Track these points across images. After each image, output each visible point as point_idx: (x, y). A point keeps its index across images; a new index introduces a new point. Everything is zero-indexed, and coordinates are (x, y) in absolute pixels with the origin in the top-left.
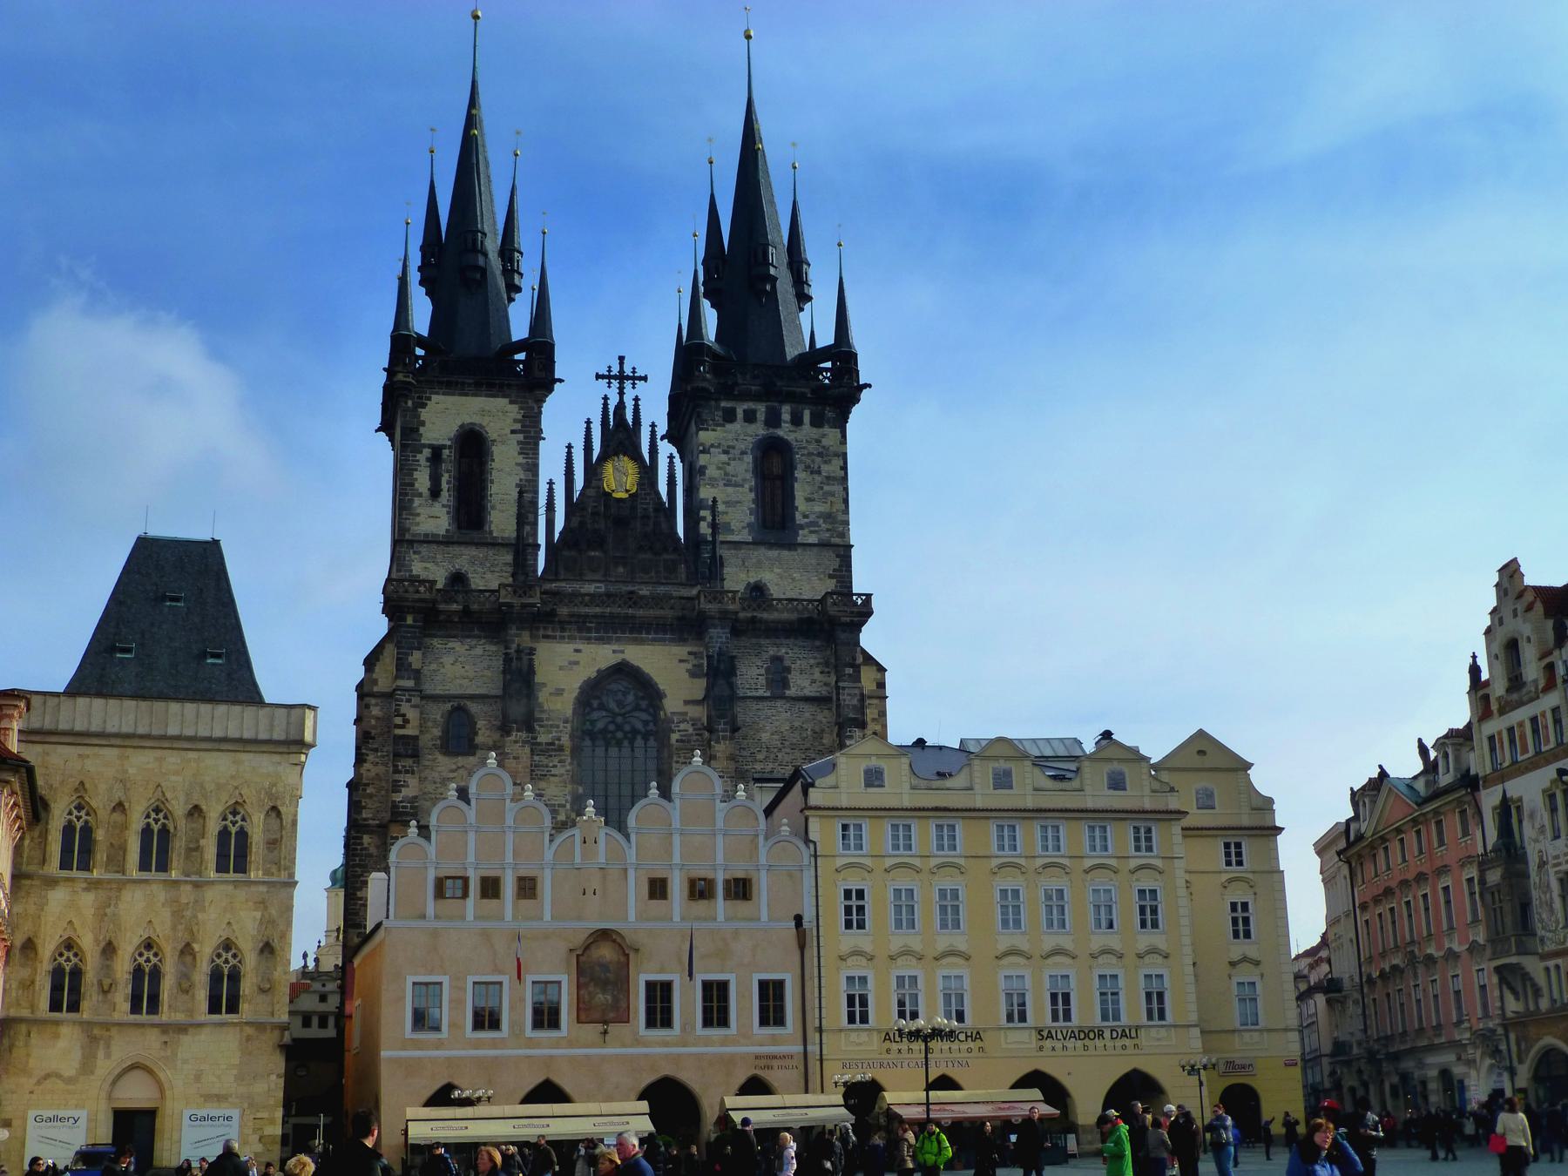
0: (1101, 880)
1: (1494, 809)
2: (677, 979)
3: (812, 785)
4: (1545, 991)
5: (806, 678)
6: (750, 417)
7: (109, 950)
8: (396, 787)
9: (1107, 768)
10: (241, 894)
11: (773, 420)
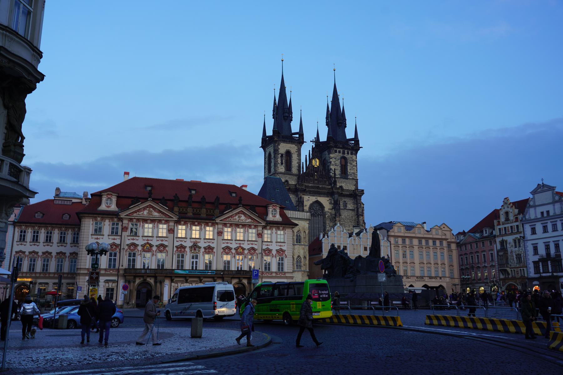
1: (499, 241)
3: (389, 231)
4: (511, 274)
5: (350, 206)
6: (339, 152)
10: (301, 247)
11: (344, 153)
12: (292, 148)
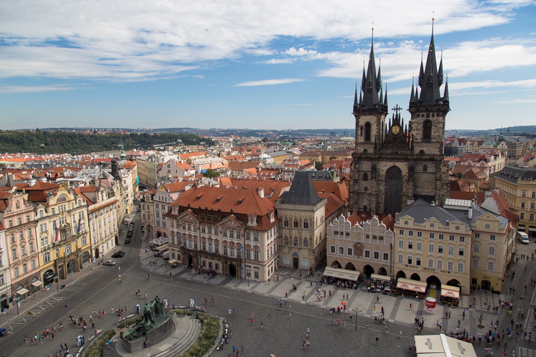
0: (451, 246)
2: (370, 251)
5: (431, 168)
6: (423, 116)
7: (291, 238)
8: (354, 188)
9: (455, 225)
10: (307, 232)
12: (372, 119)
